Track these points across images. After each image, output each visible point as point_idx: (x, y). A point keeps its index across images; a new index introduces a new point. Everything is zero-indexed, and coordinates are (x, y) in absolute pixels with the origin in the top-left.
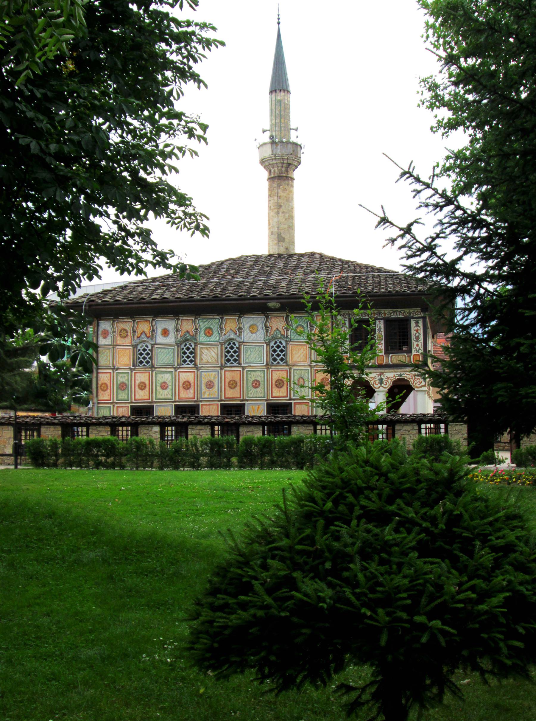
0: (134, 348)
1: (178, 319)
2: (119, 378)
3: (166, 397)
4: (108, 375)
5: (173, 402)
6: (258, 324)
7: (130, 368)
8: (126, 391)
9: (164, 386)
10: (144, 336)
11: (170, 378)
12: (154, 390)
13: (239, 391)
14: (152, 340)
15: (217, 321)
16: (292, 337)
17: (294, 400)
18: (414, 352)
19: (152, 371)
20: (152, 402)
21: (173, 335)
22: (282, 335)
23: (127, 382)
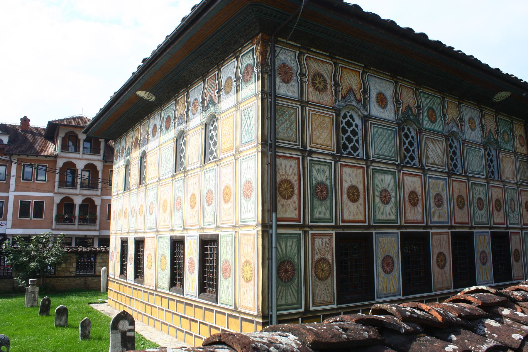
0: (338, 115)
1: (396, 83)
3: (389, 218)
4: (294, 163)
5: (398, 228)
6: (475, 119)
7: (331, 155)
8: (328, 202)
9: (385, 198)
11: (392, 184)
12: (371, 204)
13: (467, 212)
14: (364, 108)
15: (439, 101)
16: (502, 144)
17: (510, 228)
19: (368, 167)
20: (370, 227)
21: (393, 107)
22: (494, 139)
23: (328, 183)
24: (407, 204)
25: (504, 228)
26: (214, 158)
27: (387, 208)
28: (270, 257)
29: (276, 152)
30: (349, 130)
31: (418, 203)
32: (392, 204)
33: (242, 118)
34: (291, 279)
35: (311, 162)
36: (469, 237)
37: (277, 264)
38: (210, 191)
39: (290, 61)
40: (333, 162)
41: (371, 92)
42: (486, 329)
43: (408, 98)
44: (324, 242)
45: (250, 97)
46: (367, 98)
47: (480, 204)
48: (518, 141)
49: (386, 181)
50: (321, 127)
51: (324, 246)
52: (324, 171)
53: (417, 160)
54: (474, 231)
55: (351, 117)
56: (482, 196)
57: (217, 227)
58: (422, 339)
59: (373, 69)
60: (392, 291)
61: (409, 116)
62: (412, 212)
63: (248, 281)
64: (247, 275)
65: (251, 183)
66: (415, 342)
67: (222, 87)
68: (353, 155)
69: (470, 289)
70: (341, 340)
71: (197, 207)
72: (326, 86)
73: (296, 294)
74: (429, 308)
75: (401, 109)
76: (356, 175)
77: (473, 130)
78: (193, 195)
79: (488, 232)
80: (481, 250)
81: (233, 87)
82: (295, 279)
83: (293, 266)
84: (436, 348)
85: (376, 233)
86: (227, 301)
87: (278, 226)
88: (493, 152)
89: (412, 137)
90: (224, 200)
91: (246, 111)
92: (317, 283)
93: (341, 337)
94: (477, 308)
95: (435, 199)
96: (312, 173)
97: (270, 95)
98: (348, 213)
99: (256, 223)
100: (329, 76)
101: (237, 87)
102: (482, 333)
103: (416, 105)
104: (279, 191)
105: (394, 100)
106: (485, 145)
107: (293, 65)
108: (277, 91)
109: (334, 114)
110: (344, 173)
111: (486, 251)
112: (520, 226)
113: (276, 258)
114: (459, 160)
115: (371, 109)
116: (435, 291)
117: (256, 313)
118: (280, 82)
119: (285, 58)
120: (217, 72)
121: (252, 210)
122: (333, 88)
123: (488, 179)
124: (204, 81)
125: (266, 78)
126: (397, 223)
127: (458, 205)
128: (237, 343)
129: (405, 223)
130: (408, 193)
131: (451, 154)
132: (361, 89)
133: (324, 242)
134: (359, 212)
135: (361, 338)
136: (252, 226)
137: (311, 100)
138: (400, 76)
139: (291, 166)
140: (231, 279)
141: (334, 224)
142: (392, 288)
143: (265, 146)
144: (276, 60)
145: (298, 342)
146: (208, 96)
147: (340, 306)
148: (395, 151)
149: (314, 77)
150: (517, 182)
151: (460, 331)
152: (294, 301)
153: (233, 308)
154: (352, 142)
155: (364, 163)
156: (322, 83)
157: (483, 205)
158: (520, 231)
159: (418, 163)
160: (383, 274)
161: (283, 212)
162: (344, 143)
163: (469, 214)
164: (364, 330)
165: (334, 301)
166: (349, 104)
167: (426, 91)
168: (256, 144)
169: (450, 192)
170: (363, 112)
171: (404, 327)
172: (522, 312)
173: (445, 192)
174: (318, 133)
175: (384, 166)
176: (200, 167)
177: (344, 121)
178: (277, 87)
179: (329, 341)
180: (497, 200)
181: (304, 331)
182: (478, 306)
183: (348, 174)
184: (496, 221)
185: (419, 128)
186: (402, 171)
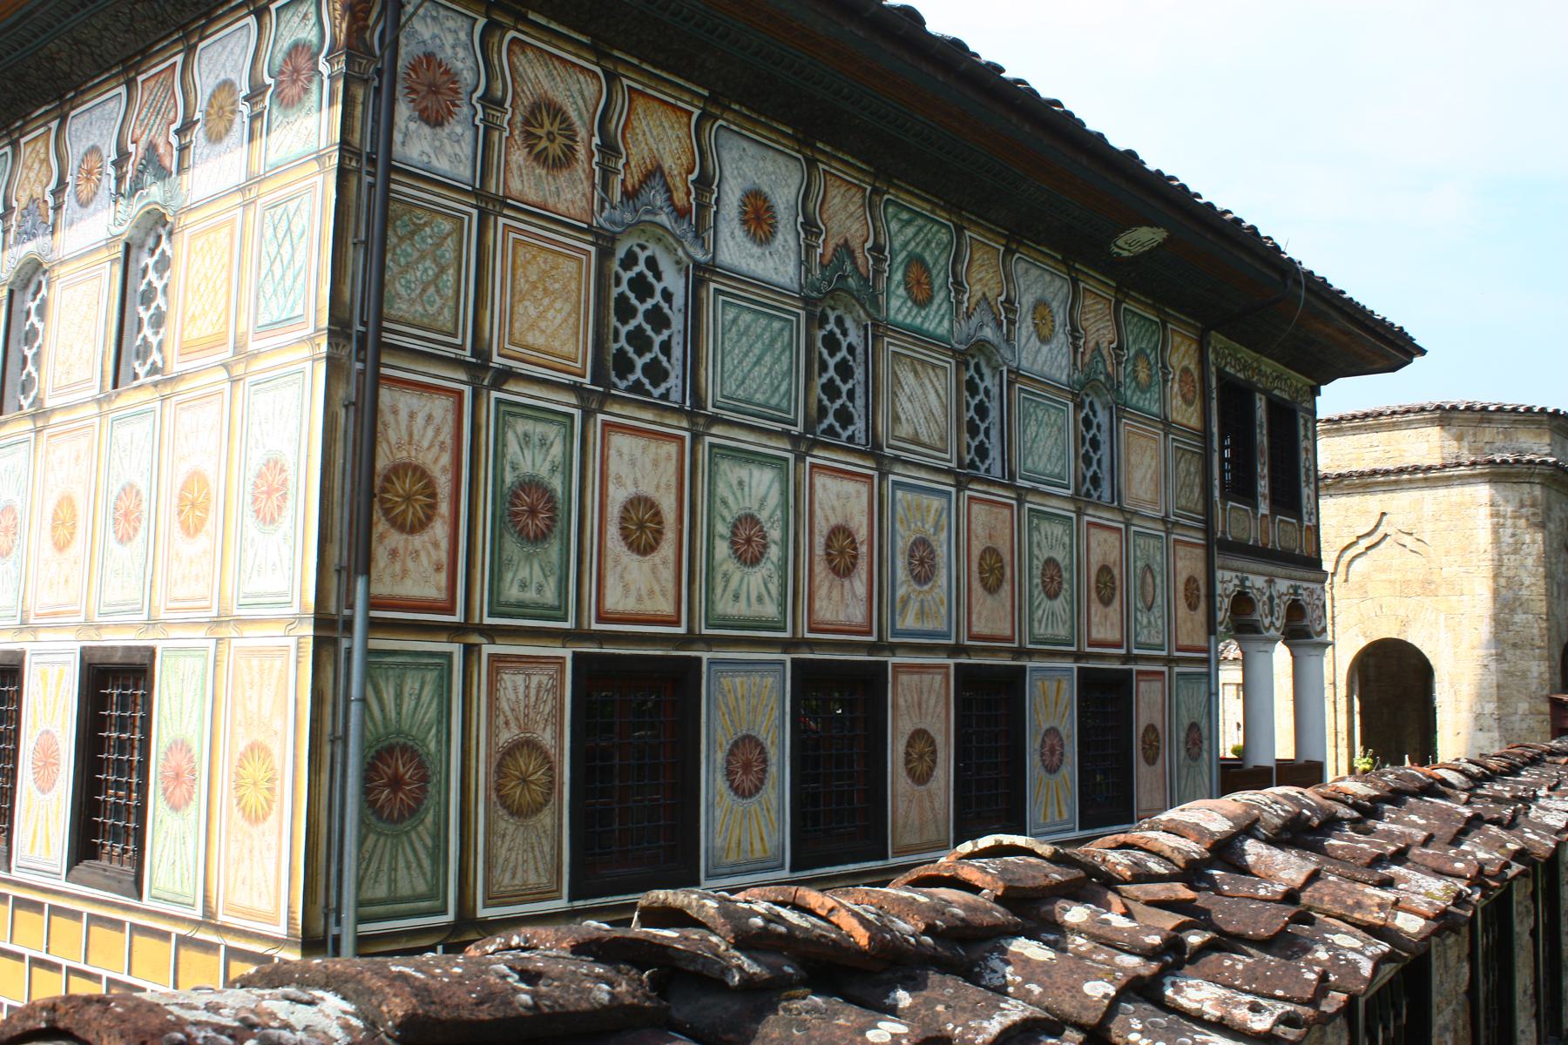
0: (605, 254)
1: (811, 163)
2: (513, 447)
3: (756, 610)
4: (440, 407)
6: (1055, 305)
7: (575, 388)
10: (659, 201)
11: (774, 499)
16: (1129, 393)
18: (1306, 523)
19: (696, 438)
20: (690, 639)
21: (792, 243)
22: (1108, 376)
23: (557, 484)
24: (821, 568)
25: (1118, 657)
26: (154, 370)
27: (752, 579)
28: (340, 732)
29: (378, 364)
30: (642, 308)
31: (854, 565)
32: (770, 565)
33: (262, 236)
34: (413, 812)
35: (502, 408)
36: (1013, 681)
37: (364, 757)
38: (129, 490)
39: (453, 47)
40: (577, 413)
41: (726, 187)
42: (1009, 969)
43: (845, 216)
44: (534, 684)
45: (299, 162)
46: (709, 206)
47: (1052, 579)
48: (1176, 386)
49: (754, 489)
50: (545, 290)
51: (533, 699)
52: (544, 443)
53: (859, 425)
54: (1029, 664)
55: (652, 263)
56: (1060, 556)
57: (152, 623)
58: (796, 1005)
59: (736, 107)
60: (758, 854)
61: (843, 278)
62: (836, 594)
63: (255, 818)
64: (254, 798)
65: (282, 470)
66: (772, 1017)
67: (198, 115)
68: (649, 394)
69: (975, 845)
70: (513, 1014)
71: (78, 548)
72: (571, 149)
73: (426, 863)
74: (830, 903)
75: (820, 251)
76: (656, 463)
77: (1044, 340)
78: (67, 502)
79: (1071, 669)
80: (1045, 726)
81: (238, 119)
82: (427, 810)
83: (421, 765)
84: (839, 1033)
85: (711, 662)
86: (178, 889)
87: (374, 625)
88: (1102, 417)
89: (851, 349)
90: (182, 523)
91: (280, 210)
92: (503, 825)
93: (511, 1003)
94: (989, 904)
95: (912, 556)
96: (504, 445)
97: (372, 162)
98: (620, 589)
99: (295, 609)
100: (586, 116)
101: (254, 118)
102: (997, 982)
103: (869, 245)
104: (383, 501)
105: (800, 219)
106: (1080, 392)
107: (460, 65)
108: (397, 148)
109: (592, 249)
110: (613, 452)
111: (1061, 729)
112: (1164, 653)
113: (362, 736)
114: (994, 433)
115: (721, 243)
116: (897, 854)
117: (281, 931)
118: (410, 119)
119: (434, 37)
120: (179, 58)
121: (281, 562)
122: (596, 159)
123: (1082, 500)
124: (130, 84)
125: (360, 99)
126: (784, 629)
127: (982, 580)
128: (115, 1031)
129: (811, 630)
130: (825, 532)
131: (972, 413)
132: (690, 172)
133: (534, 684)
134: (657, 588)
135: (584, 1006)
136: (278, 620)
137: (514, 193)
138: (826, 143)
139: (429, 418)
140: (195, 812)
141: (569, 624)
142: (757, 845)
143: (342, 341)
144: (402, 40)
145: (355, 1022)
146: (142, 144)
147: (579, 904)
148: (789, 391)
149: (532, 113)
150: (1167, 515)
151: (926, 978)
152: (422, 887)
153: (197, 914)
154: (649, 348)
155: (685, 424)
156: (560, 139)
157: (1060, 583)
158: (1165, 669)
159: (863, 435)
160: (729, 798)
161: (393, 576)
162: (621, 351)
163: (1017, 611)
164: (599, 978)
165: (559, 889)
166: (647, 218)
167: (904, 198)
168: (311, 330)
169: (961, 534)
170: (691, 250)
171: (740, 968)
172: (1124, 915)
173: (944, 535)
174: (532, 311)
175: (751, 437)
176: (99, 401)
177: (626, 276)
178: (398, 137)
179: (465, 1014)
180: (1105, 570)
181: (376, 983)
182: (997, 900)
183: (626, 458)
184: (1097, 634)
185: (873, 319)
186: (809, 459)
